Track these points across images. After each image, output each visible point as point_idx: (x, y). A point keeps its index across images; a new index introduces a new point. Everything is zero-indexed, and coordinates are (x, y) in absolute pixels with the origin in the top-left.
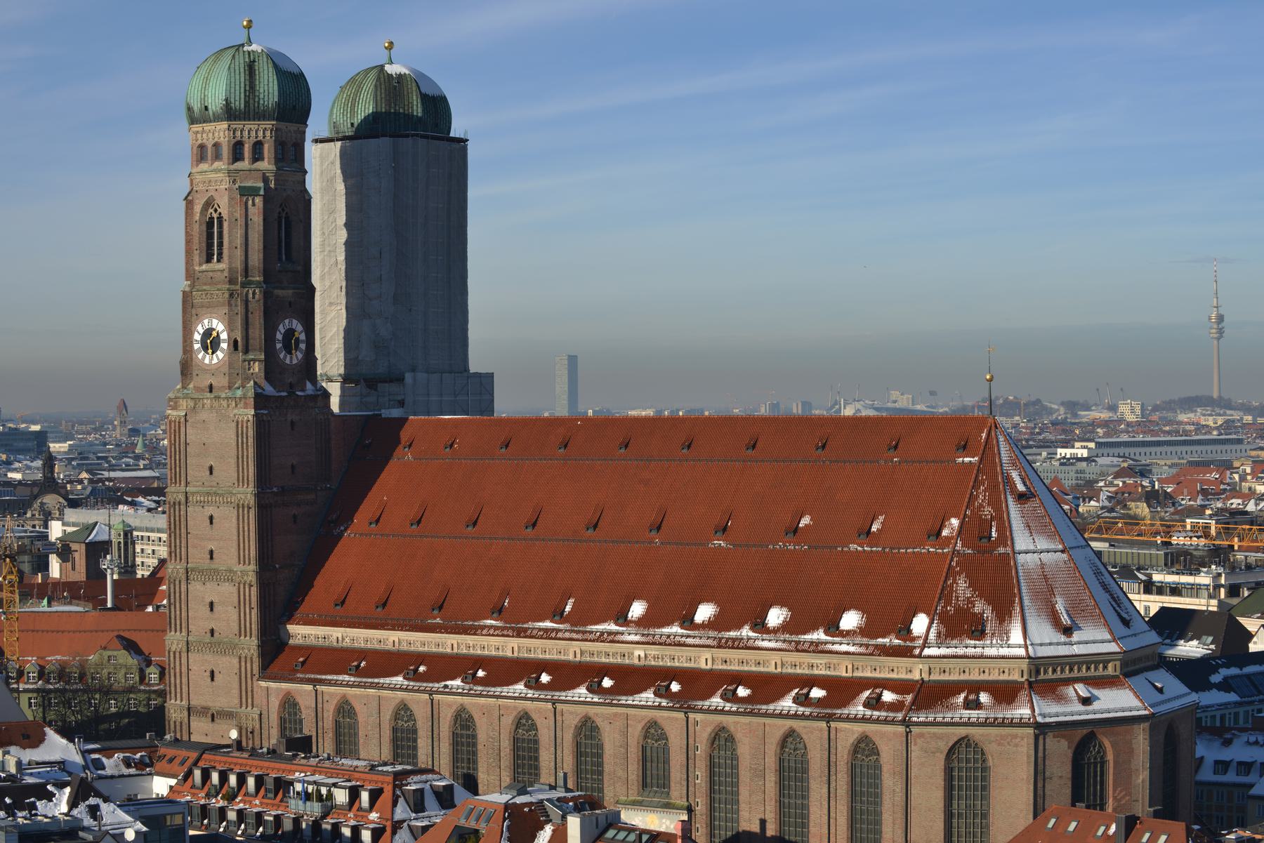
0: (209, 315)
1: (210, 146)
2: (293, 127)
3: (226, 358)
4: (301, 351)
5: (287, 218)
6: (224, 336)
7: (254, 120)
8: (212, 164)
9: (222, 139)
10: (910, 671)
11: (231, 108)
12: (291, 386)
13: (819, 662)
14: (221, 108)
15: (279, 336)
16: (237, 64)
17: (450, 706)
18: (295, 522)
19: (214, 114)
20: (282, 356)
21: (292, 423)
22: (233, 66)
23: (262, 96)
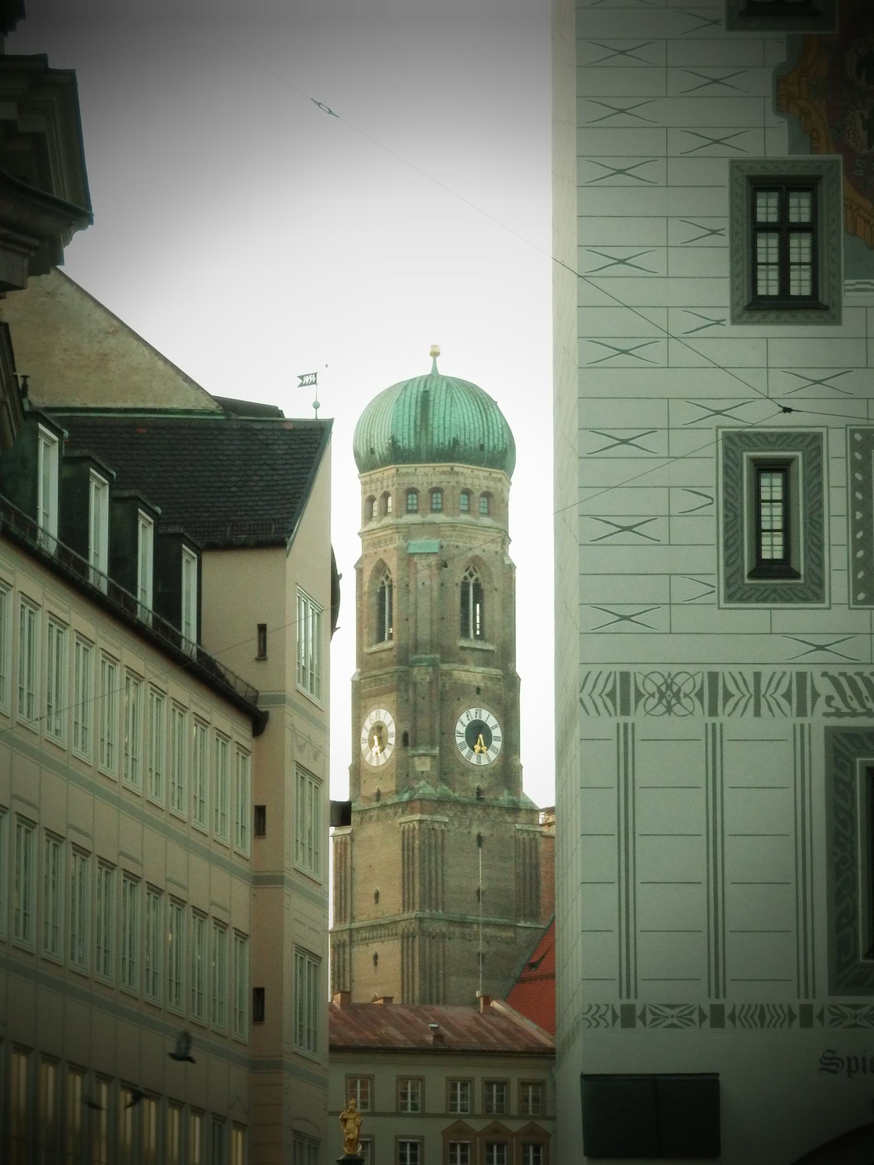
0: (376, 706)
1: (378, 495)
2: (482, 472)
3: (394, 756)
4: (494, 750)
5: (477, 586)
6: (392, 729)
7: (427, 462)
9: (390, 487)
11: (399, 448)
12: (479, 792)
14: (387, 450)
15: (461, 728)
16: (408, 394)
19: (380, 456)
21: (480, 839)
22: (403, 397)
23: (436, 432)
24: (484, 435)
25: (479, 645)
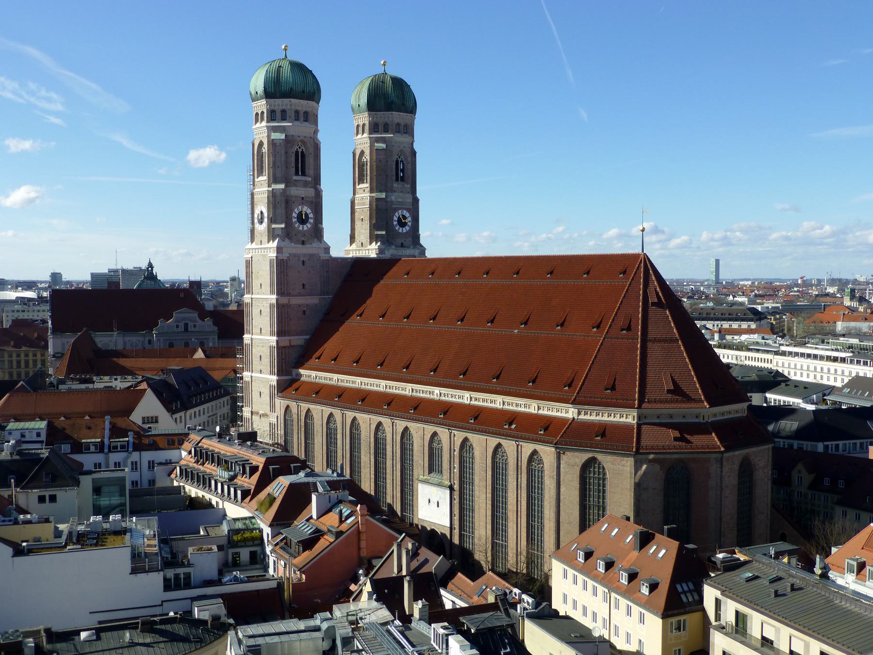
4: (310, 223)
8: (261, 123)
10: (568, 412)
13: (521, 402)
15: (295, 215)
17: (350, 417)
18: (304, 314)
20: (296, 225)
22: (269, 69)
23: (283, 85)
24: (304, 86)
25: (303, 178)
